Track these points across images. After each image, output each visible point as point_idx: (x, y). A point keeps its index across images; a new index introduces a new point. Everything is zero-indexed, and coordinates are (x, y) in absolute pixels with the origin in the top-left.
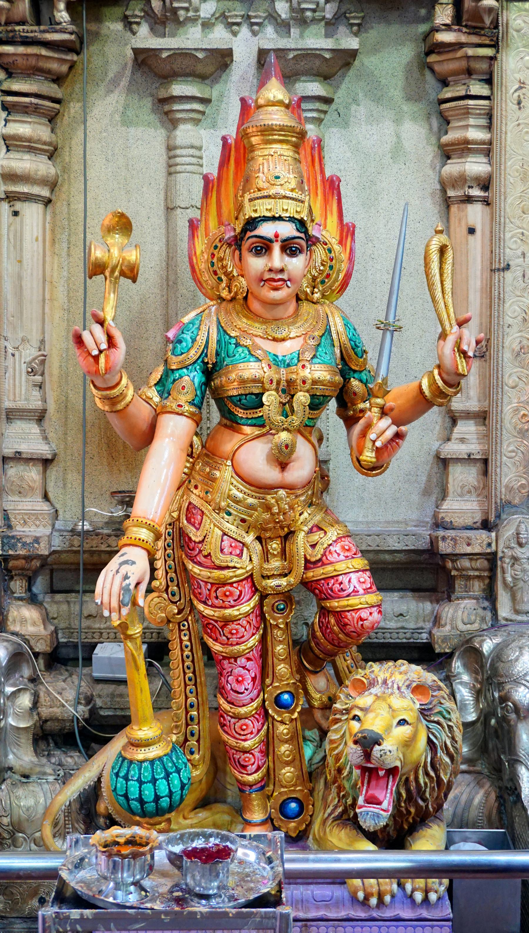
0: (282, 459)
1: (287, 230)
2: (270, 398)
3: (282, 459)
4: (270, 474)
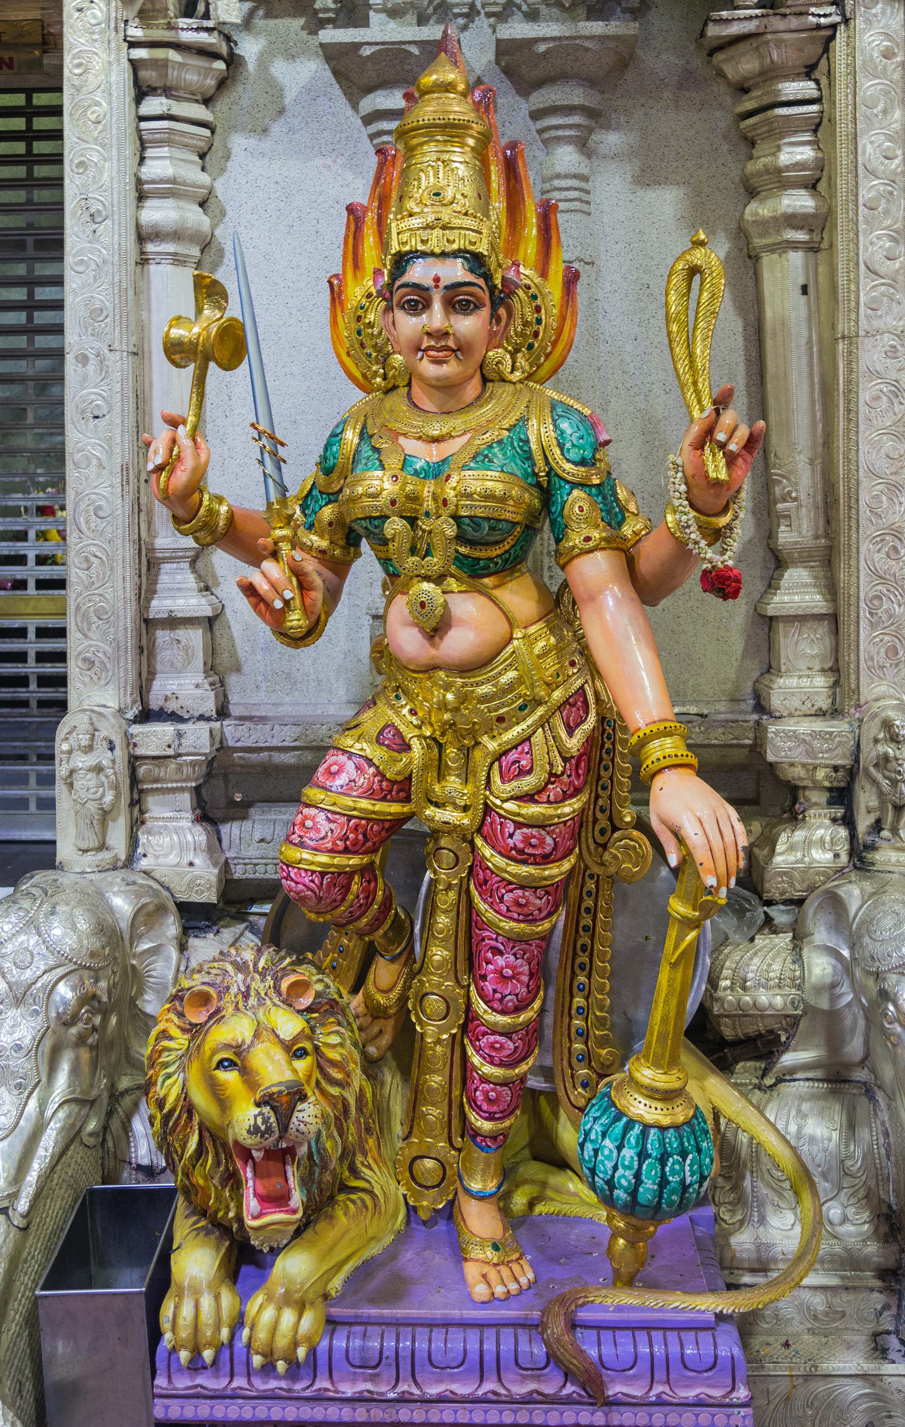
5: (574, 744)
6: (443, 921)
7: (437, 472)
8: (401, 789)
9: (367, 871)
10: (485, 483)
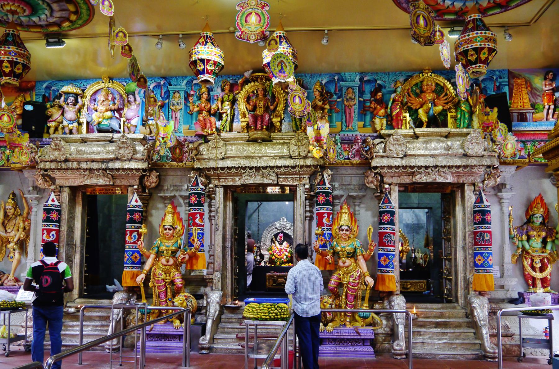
0: (168, 261)
1: (169, 227)
2: (165, 252)
3: (168, 261)
4: (165, 263)
5: (358, 275)
6: (344, 294)
7: (345, 247)
8: (340, 279)
9: (336, 287)
10: (348, 249)
